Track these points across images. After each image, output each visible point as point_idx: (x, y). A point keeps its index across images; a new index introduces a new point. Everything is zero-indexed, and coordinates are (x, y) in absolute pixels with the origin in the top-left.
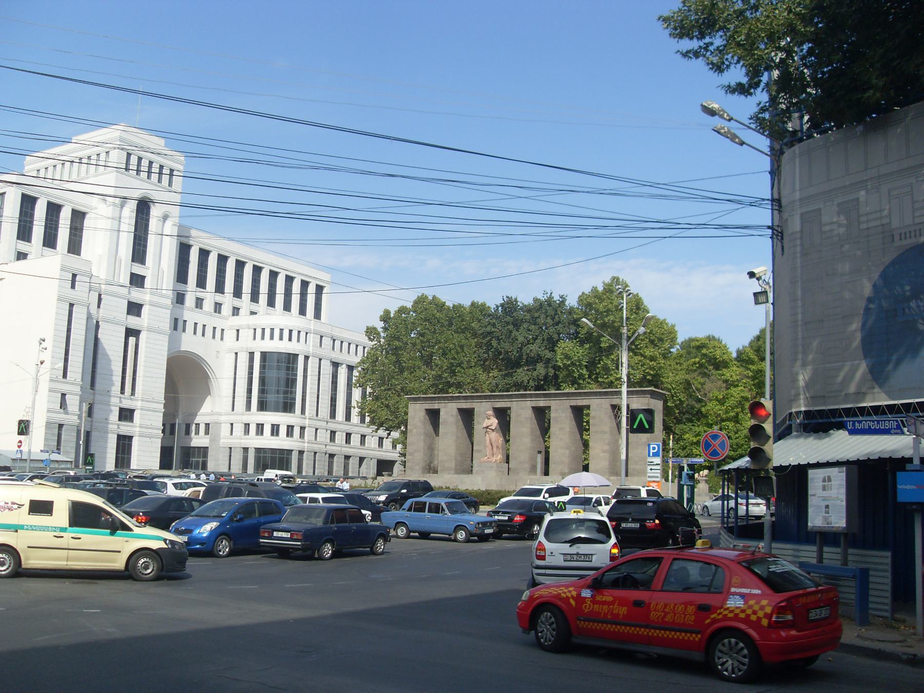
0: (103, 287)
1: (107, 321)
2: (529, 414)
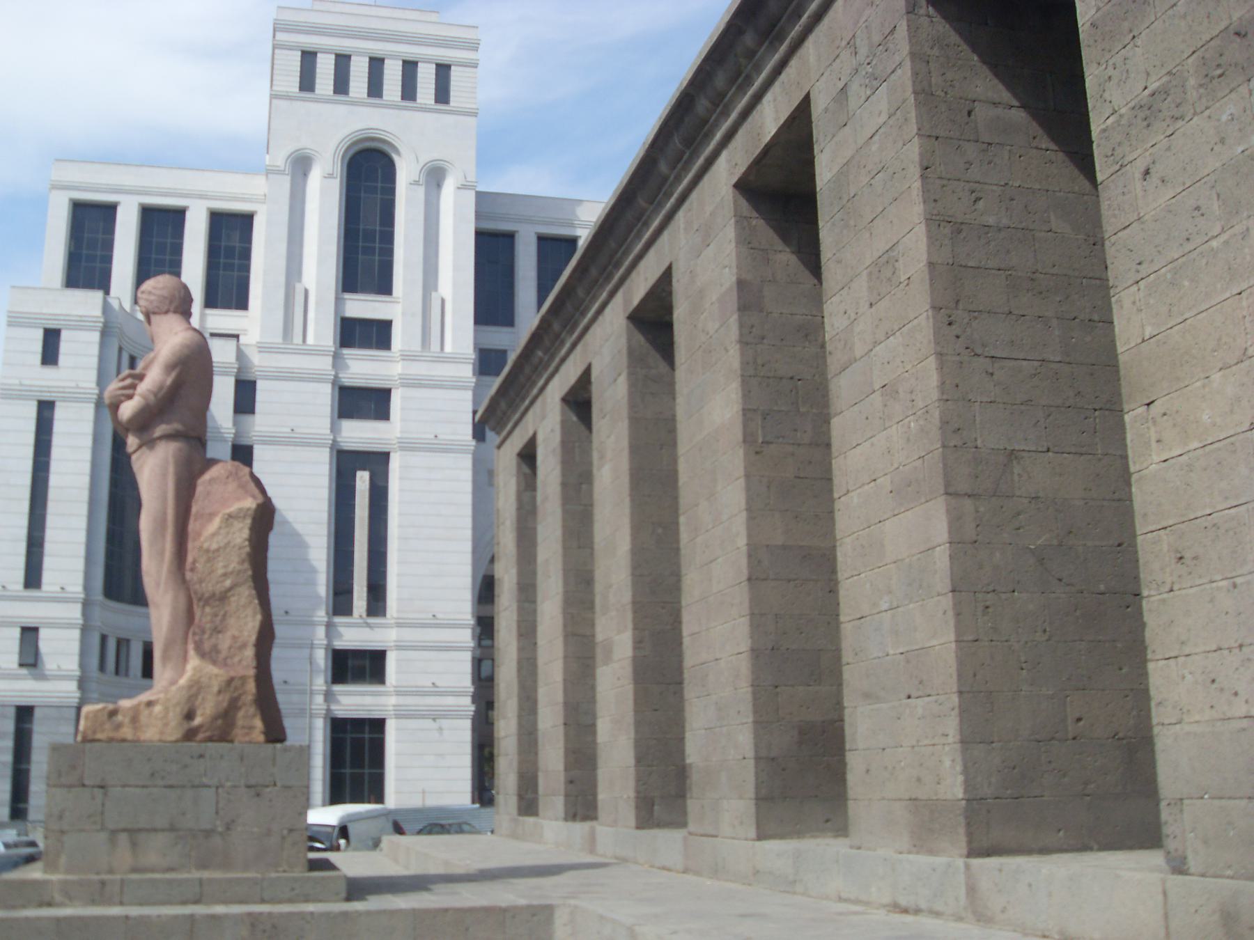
0: (257, 360)
1: (273, 441)
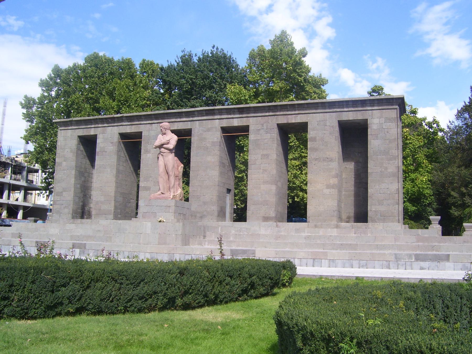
2: (216, 137)
